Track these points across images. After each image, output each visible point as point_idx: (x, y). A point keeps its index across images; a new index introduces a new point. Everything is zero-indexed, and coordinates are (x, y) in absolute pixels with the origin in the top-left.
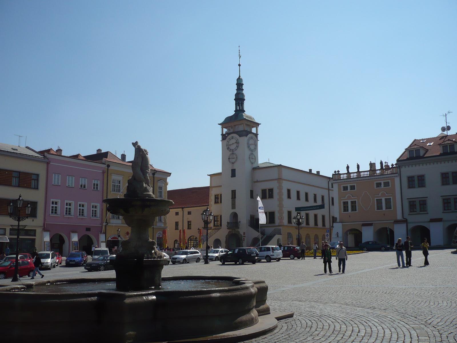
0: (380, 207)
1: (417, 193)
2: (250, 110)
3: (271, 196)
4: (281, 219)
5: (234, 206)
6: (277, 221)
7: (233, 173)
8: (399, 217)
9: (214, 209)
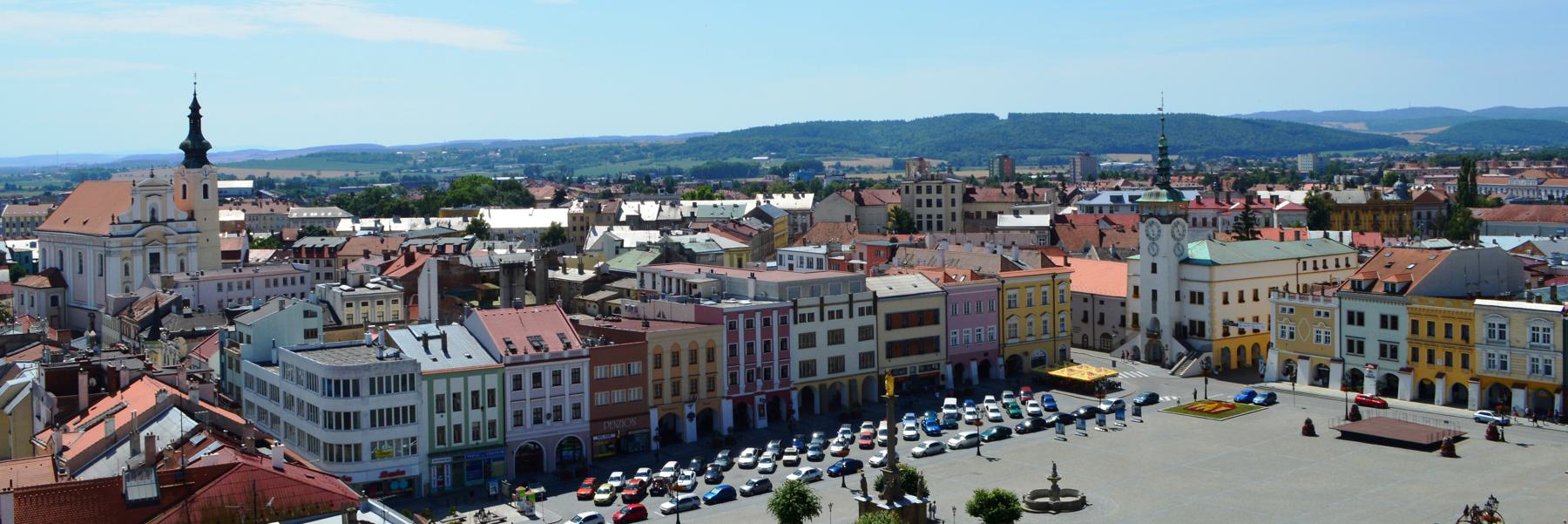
0: (1318, 339)
3: (1201, 302)
4: (1212, 330)
5: (1154, 310)
6: (1208, 334)
7: (1154, 268)
8: (1337, 356)
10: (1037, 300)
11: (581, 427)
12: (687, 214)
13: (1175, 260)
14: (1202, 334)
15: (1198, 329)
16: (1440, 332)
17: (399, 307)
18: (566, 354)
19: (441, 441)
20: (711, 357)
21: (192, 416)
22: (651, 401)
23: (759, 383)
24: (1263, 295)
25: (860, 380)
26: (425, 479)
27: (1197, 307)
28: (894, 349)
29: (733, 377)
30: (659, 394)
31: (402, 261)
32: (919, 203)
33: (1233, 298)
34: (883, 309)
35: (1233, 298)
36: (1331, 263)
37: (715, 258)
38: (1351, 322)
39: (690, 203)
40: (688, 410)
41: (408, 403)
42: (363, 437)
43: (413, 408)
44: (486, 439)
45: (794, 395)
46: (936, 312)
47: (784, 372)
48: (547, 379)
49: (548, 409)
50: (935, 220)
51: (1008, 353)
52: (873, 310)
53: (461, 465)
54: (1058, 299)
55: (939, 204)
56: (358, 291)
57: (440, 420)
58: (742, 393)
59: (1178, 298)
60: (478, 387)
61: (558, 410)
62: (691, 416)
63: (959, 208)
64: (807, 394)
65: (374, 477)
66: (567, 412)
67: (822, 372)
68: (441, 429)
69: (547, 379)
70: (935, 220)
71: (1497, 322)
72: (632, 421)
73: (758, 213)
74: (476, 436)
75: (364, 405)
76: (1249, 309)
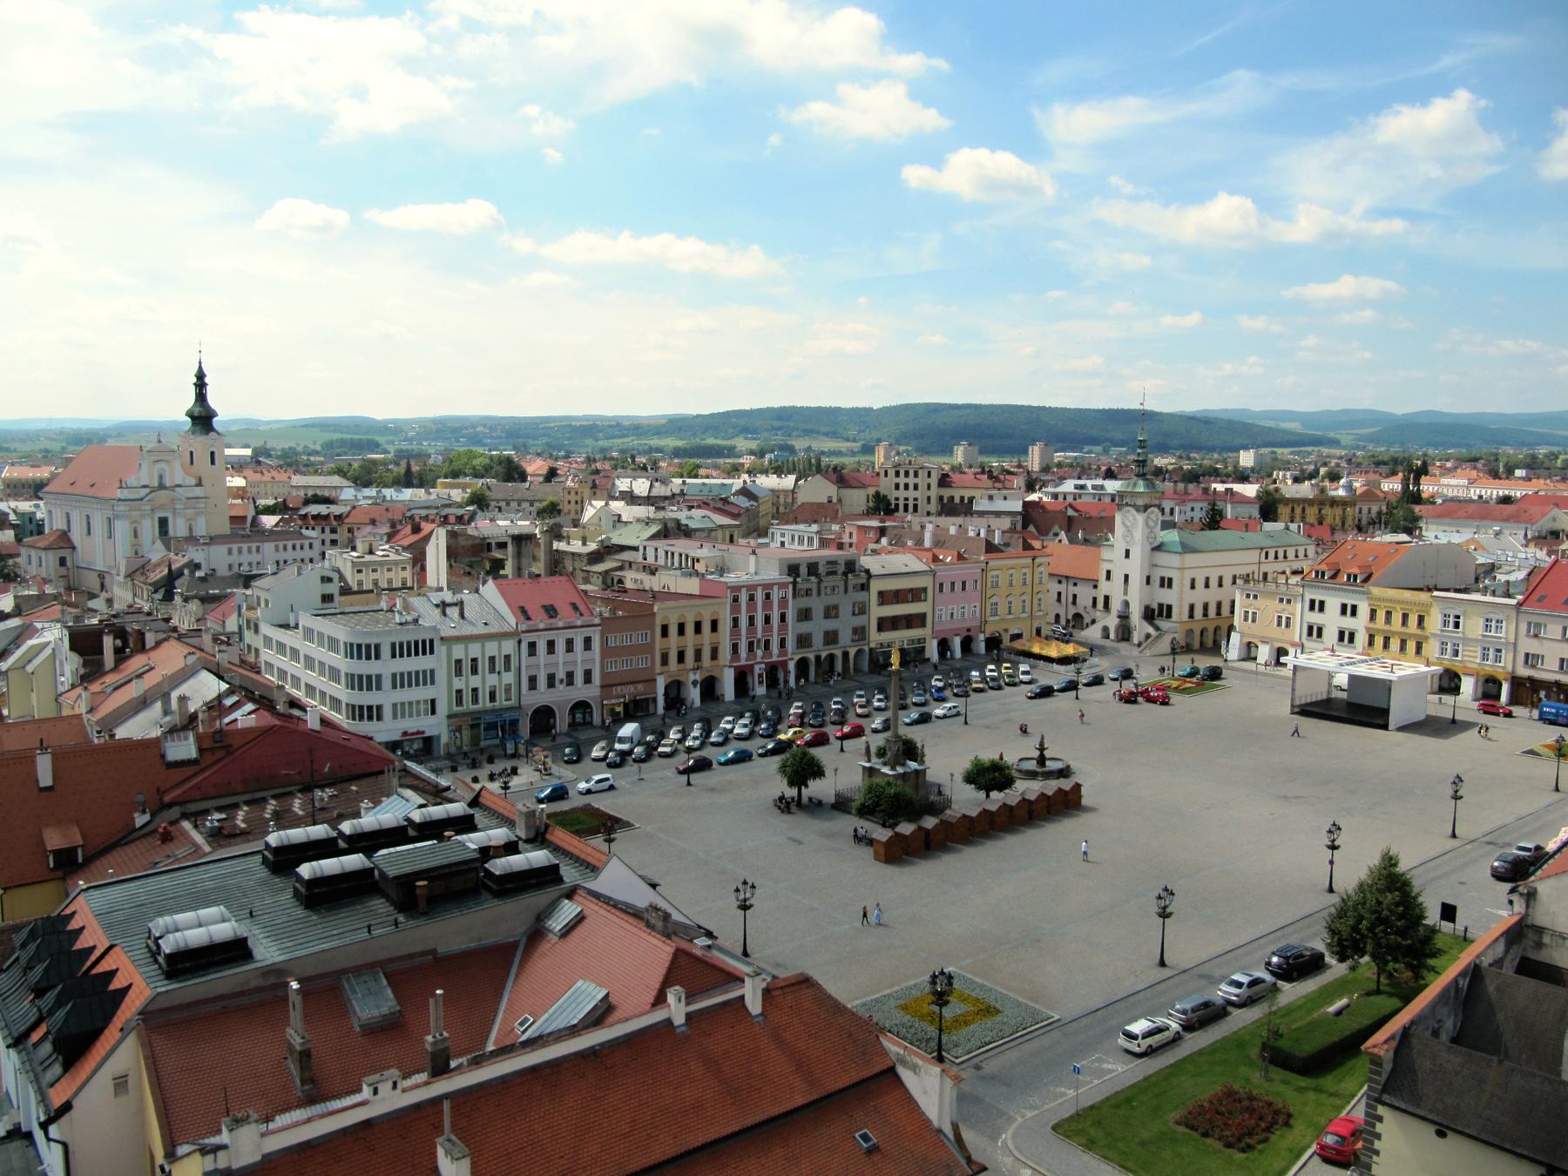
0: (1279, 624)
1: (1315, 618)
3: (1170, 586)
5: (1126, 593)
8: (1297, 639)
9: (1105, 588)
10: (1017, 581)
11: (590, 693)
12: (676, 491)
13: (1149, 548)
14: (1169, 615)
15: (1166, 611)
17: (408, 574)
18: (579, 623)
19: (459, 702)
20: (714, 626)
21: (221, 678)
22: (658, 668)
23: (759, 653)
24: (1227, 581)
25: (852, 652)
26: (444, 739)
27: (1165, 590)
28: (885, 624)
29: (735, 647)
30: (665, 660)
31: (408, 529)
32: (897, 487)
33: (1200, 584)
34: (876, 587)
35: (1200, 584)
36: (1291, 554)
37: (709, 534)
38: (1312, 608)
39: (680, 481)
40: (692, 677)
41: (428, 667)
42: (385, 698)
43: (432, 671)
44: (501, 702)
45: (791, 666)
46: (925, 590)
47: (783, 643)
48: (560, 646)
49: (561, 675)
50: (911, 503)
51: (990, 630)
52: (865, 587)
53: (478, 725)
54: (1036, 581)
55: (916, 487)
56: (368, 558)
57: (458, 683)
58: (743, 662)
59: (1148, 582)
60: (495, 653)
61: (570, 676)
62: (695, 683)
63: (934, 492)
64: (802, 665)
65: (396, 737)
66: (579, 678)
68: (459, 692)
69: (560, 646)
70: (911, 503)
71: (1452, 613)
72: (640, 687)
73: (745, 492)
74: (492, 697)
75: (387, 666)
76: (1212, 596)
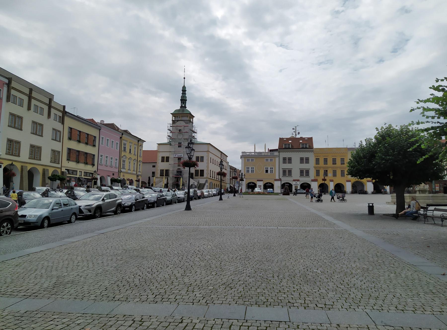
0: (267, 171)
2: (189, 108)
8: (277, 178)
16: (330, 162)
34: (69, 122)
67: (25, 154)
